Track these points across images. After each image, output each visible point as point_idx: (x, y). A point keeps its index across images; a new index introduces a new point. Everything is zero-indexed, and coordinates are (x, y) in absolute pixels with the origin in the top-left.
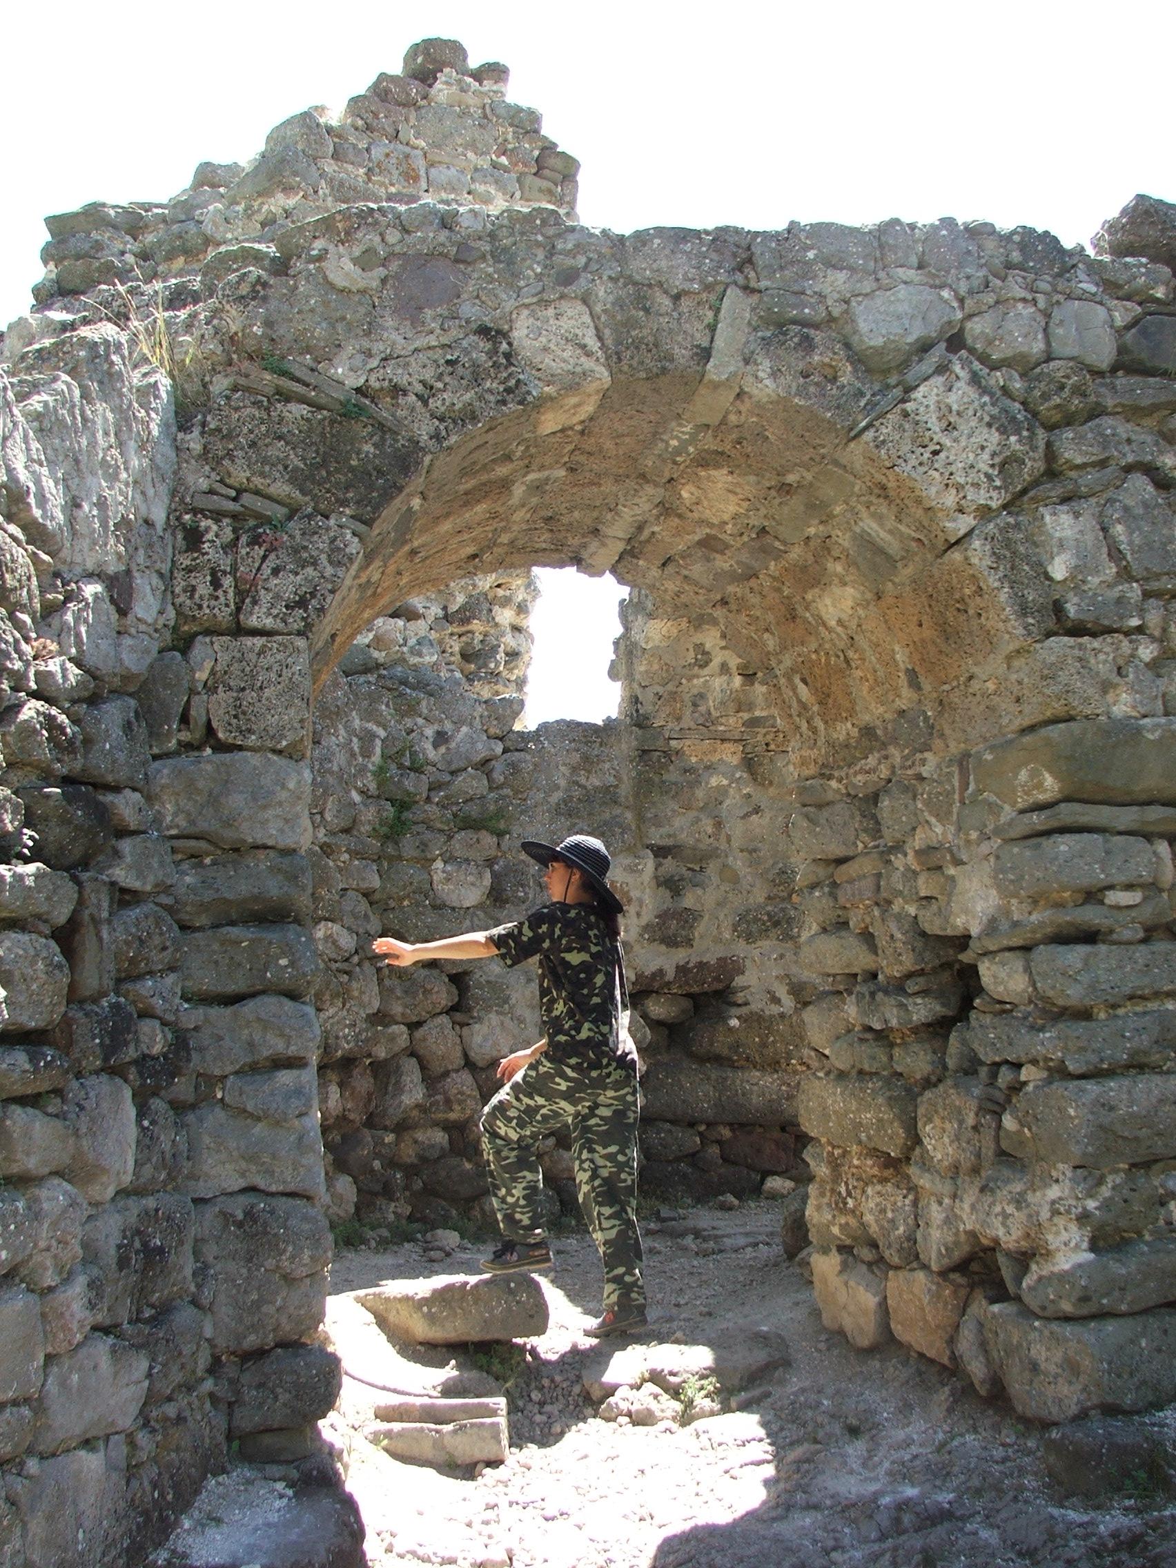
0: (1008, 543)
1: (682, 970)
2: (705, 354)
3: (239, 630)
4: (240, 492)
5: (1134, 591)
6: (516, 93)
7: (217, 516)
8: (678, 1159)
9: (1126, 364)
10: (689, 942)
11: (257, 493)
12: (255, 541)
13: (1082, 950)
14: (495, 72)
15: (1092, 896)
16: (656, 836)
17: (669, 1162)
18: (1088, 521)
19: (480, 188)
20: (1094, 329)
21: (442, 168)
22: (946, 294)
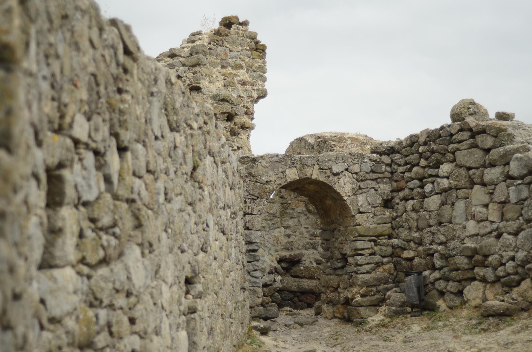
0: (352, 201)
1: (290, 255)
2: (312, 175)
3: (252, 214)
4: (251, 195)
5: (370, 207)
6: (251, 28)
7: (249, 199)
8: (288, 300)
9: (372, 171)
10: (292, 249)
11: (253, 195)
12: (254, 202)
13: (360, 257)
14: (245, 24)
16: (285, 224)
17: (286, 300)
20: (368, 166)
21: (233, 52)
22: (346, 164)
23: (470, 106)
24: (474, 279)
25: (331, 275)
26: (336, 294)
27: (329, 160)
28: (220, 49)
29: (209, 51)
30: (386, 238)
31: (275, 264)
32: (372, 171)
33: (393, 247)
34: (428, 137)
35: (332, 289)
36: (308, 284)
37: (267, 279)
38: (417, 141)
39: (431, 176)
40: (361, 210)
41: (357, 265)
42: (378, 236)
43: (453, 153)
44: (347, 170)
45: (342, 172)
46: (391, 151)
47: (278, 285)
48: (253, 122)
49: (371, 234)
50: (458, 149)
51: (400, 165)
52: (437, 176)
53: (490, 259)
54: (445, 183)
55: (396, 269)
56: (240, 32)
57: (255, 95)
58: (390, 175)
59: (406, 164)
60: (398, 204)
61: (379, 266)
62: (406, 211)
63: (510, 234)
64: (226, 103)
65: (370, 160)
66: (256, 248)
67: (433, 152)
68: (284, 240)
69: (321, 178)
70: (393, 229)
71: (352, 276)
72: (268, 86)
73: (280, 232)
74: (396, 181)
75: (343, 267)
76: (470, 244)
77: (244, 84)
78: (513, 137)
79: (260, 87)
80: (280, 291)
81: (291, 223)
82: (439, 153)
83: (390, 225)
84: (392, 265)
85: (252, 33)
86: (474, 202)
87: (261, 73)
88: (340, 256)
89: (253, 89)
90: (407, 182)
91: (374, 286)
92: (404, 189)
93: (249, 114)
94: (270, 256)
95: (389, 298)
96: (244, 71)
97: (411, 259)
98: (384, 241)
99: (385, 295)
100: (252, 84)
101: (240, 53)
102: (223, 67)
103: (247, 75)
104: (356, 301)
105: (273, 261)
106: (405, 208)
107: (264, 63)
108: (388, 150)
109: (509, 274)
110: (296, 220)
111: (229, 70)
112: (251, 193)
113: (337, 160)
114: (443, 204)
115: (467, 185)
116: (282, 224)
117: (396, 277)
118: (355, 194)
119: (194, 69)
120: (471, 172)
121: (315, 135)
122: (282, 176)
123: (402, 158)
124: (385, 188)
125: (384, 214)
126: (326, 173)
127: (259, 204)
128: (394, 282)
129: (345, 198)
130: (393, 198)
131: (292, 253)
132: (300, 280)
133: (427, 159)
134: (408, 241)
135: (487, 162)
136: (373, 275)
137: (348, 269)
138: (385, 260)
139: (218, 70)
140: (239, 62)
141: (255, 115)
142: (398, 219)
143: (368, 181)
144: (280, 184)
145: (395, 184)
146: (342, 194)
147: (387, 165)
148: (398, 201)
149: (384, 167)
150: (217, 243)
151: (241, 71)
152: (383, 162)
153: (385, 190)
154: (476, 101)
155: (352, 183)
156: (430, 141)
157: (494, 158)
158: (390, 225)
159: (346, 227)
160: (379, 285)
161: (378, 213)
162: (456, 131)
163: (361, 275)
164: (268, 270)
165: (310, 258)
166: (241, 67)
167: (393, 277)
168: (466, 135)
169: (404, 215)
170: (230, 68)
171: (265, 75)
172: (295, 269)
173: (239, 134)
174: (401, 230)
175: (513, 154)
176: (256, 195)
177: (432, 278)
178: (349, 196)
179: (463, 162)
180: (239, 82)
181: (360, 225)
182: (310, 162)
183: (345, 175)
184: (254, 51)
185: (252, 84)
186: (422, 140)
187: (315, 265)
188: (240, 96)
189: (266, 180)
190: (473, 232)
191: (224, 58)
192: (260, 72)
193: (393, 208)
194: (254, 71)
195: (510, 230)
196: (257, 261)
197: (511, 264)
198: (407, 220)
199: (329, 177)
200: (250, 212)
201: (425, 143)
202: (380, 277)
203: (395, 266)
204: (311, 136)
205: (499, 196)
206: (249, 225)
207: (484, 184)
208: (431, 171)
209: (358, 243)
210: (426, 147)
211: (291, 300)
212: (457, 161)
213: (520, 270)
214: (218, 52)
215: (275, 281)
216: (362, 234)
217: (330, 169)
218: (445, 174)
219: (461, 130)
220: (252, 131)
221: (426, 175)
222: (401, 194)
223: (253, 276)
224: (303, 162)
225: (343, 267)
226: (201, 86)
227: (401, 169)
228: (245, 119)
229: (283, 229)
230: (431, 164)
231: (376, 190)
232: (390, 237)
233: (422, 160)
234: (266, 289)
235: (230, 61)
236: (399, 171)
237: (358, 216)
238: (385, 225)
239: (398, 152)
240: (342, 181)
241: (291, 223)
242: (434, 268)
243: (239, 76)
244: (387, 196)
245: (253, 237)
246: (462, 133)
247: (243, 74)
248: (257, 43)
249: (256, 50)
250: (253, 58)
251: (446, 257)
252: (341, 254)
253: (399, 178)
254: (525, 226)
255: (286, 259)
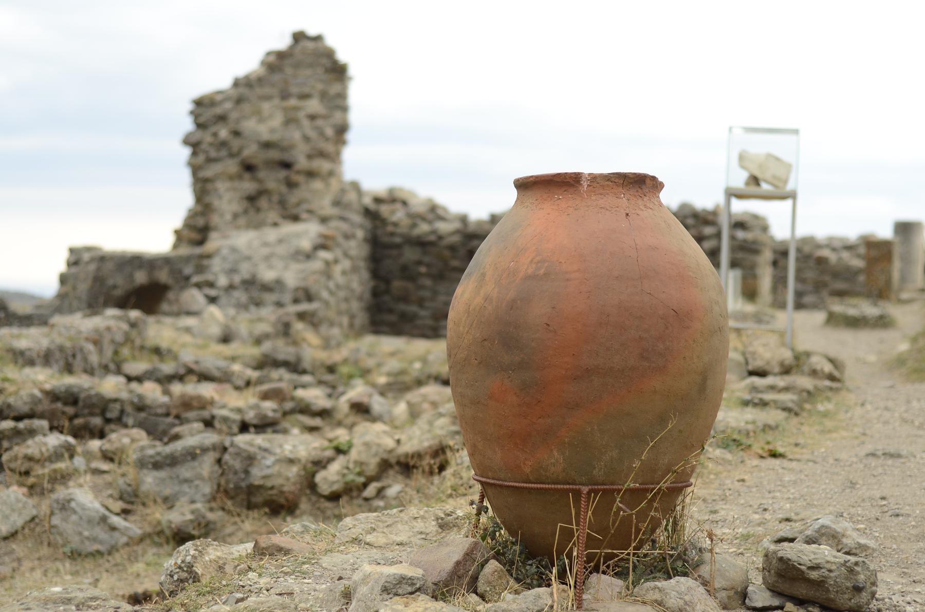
57: (329, 132)
77: (312, 117)
101: (311, 79)
111: (293, 102)
192: (337, 102)
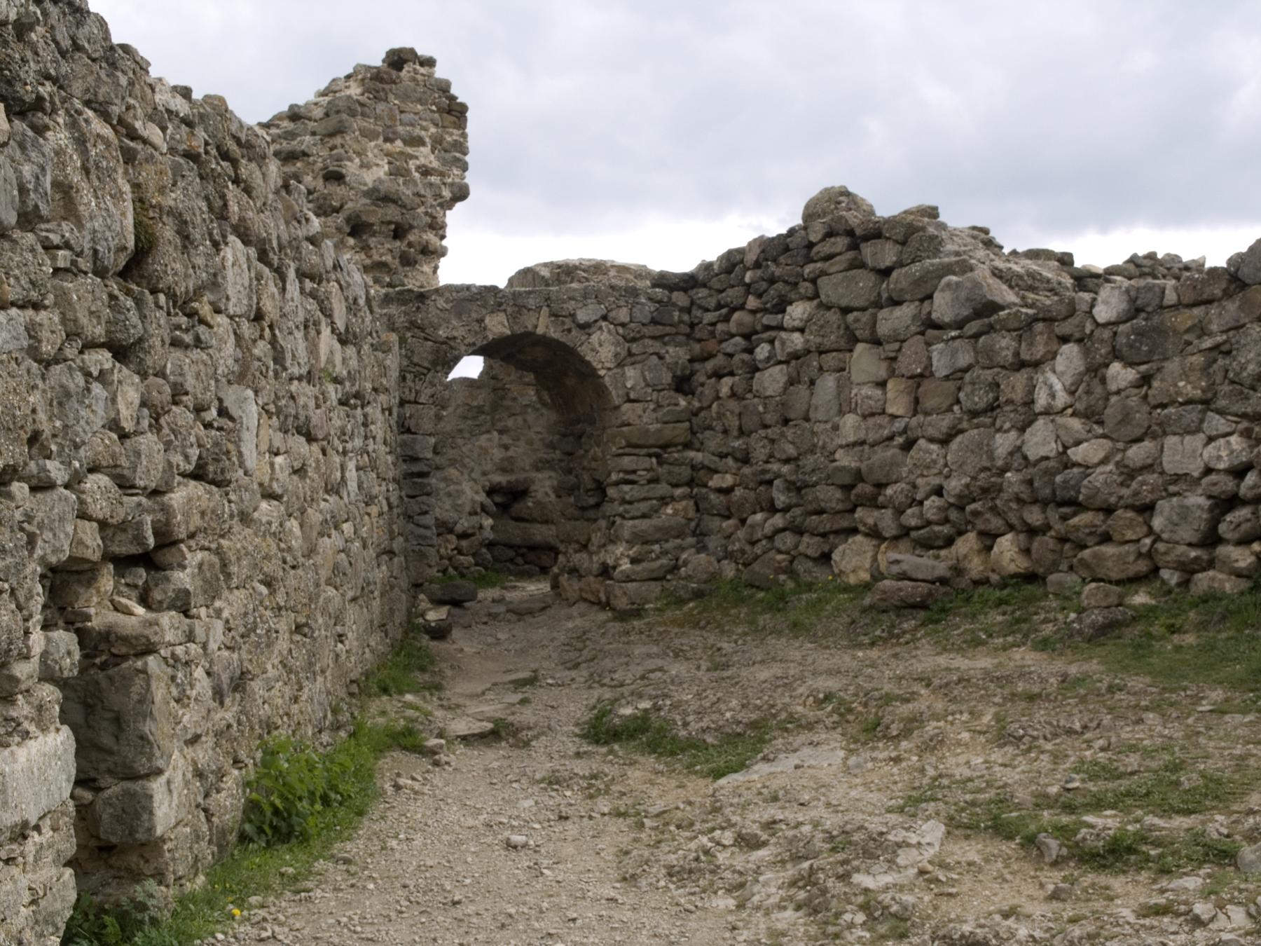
1: (509, 482)
2: (536, 327)
3: (416, 402)
4: (416, 365)
5: (650, 390)
6: (440, 72)
9: (654, 322)
10: (512, 470)
14: (429, 62)
15: (634, 472)
16: (500, 425)
18: (639, 372)
19: (424, 123)
23: (841, 198)
24: (854, 531)
25: (576, 519)
26: (585, 555)
27: (570, 299)
28: (381, 107)
29: (359, 109)
30: (678, 451)
31: (482, 497)
32: (654, 322)
33: (693, 467)
34: (763, 251)
35: (577, 546)
36: (541, 533)
37: (466, 524)
38: (742, 261)
39: (768, 328)
40: (632, 396)
41: (624, 502)
42: (665, 447)
43: (813, 282)
44: (604, 318)
45: (596, 321)
46: (687, 283)
47: (488, 534)
48: (444, 243)
49: (651, 442)
50: (824, 273)
51: (707, 310)
52: (781, 328)
53: (889, 491)
54: (797, 340)
55: (698, 510)
56: (419, 77)
57: (447, 193)
58: (688, 330)
59: (719, 307)
60: (702, 385)
61: (667, 504)
62: (718, 398)
63: (931, 440)
64: (392, 206)
65: (650, 299)
66: (426, 469)
67: (772, 281)
68: (498, 454)
69: (554, 333)
70: (694, 433)
71: (614, 522)
72: (470, 178)
73: (489, 440)
74: (699, 341)
75: (597, 505)
76: (845, 460)
77: (426, 172)
78: (940, 243)
79: (457, 180)
80: (491, 545)
81: (510, 423)
82: (786, 282)
83: (687, 424)
84: (692, 503)
85: (440, 81)
86: (855, 377)
87: (458, 155)
88: (591, 485)
89: (444, 184)
90: (721, 342)
91: (657, 542)
92: (715, 356)
93: (438, 228)
94: (472, 483)
95: (685, 564)
96: (426, 150)
97: (727, 491)
98: (676, 455)
99: (677, 560)
100: (442, 174)
102: (386, 140)
103: (432, 157)
104: (622, 572)
105: (477, 493)
106: (717, 392)
107: (464, 136)
108: (685, 281)
109: (929, 523)
110: (520, 419)
112: (416, 360)
113: (585, 298)
114: (792, 382)
115: (842, 344)
116: (493, 425)
117: (698, 525)
118: (620, 365)
119: (332, 141)
120: (851, 317)
121: (552, 263)
122: (477, 328)
123: (711, 296)
124: (677, 354)
125: (677, 405)
126: (563, 323)
127: (430, 382)
128: (694, 534)
129: (602, 373)
130: (693, 373)
131: (512, 478)
132: (527, 525)
133: (760, 296)
134: (722, 456)
135: (885, 296)
136: (655, 521)
137: (608, 508)
138: (678, 492)
139: (376, 146)
140: (417, 131)
141: (449, 232)
142: (702, 414)
143: (647, 341)
144: (474, 344)
145: (697, 348)
146: (594, 364)
147: (682, 310)
148: (703, 379)
149: (676, 314)
150: (279, 460)
151: (422, 149)
152: (674, 305)
153: (680, 358)
154: (851, 189)
155: (617, 344)
156: (767, 260)
157: (899, 286)
158: (687, 424)
159: (604, 428)
160: (667, 541)
161: (665, 403)
162: (819, 236)
163: (631, 522)
164: (468, 508)
165: (544, 486)
166: (420, 142)
167: (693, 524)
168: (841, 242)
169: (715, 405)
170: (399, 143)
171: (467, 158)
172: (517, 508)
173: (416, 262)
174: (708, 433)
175: (941, 277)
176: (426, 364)
177: (768, 529)
178: (609, 369)
179: (834, 299)
180: (418, 168)
181: (629, 425)
182: (531, 302)
183: (600, 328)
184: (445, 115)
185: (442, 174)
186: (751, 258)
187: (553, 496)
188: (418, 195)
189: (445, 335)
190: (852, 439)
191: (389, 123)
193: (693, 394)
194: (446, 151)
195: (931, 432)
196: (428, 494)
197: (933, 502)
198: (720, 416)
199: (569, 330)
200: (412, 399)
201: (757, 265)
202: (667, 524)
203: (696, 504)
204: (545, 265)
205: (910, 361)
206: (412, 424)
207: (877, 342)
208: (768, 319)
209: (626, 459)
210: (759, 272)
211: (511, 560)
212: (823, 297)
213: (954, 515)
214: (378, 111)
215: (481, 527)
216: (634, 441)
217: (573, 316)
218: (797, 323)
219: (830, 234)
220: (442, 259)
221: (759, 328)
222: (710, 365)
223: (418, 525)
224: (520, 302)
225: (597, 505)
226: (344, 171)
227: (709, 317)
228: (430, 236)
229: (495, 434)
230: (768, 305)
231: (661, 358)
232: (687, 446)
233: (751, 298)
234: (464, 543)
235: (400, 129)
236: (705, 322)
237: (627, 406)
238: (678, 425)
239: (704, 285)
240: (595, 338)
241: (510, 423)
242: (772, 509)
243: (417, 158)
244: (682, 370)
245: (418, 447)
246: (833, 239)
247: (425, 156)
248: (453, 98)
249: (449, 112)
250: (443, 127)
251: (796, 488)
252: (594, 480)
253: (705, 335)
254: (965, 425)
255: (502, 488)
